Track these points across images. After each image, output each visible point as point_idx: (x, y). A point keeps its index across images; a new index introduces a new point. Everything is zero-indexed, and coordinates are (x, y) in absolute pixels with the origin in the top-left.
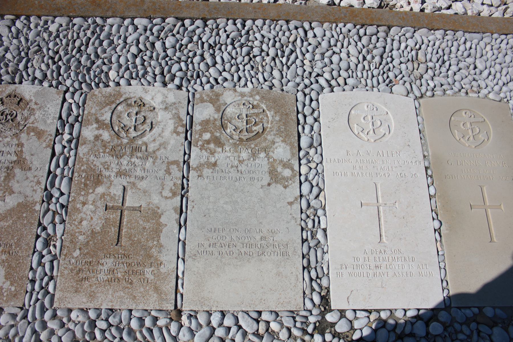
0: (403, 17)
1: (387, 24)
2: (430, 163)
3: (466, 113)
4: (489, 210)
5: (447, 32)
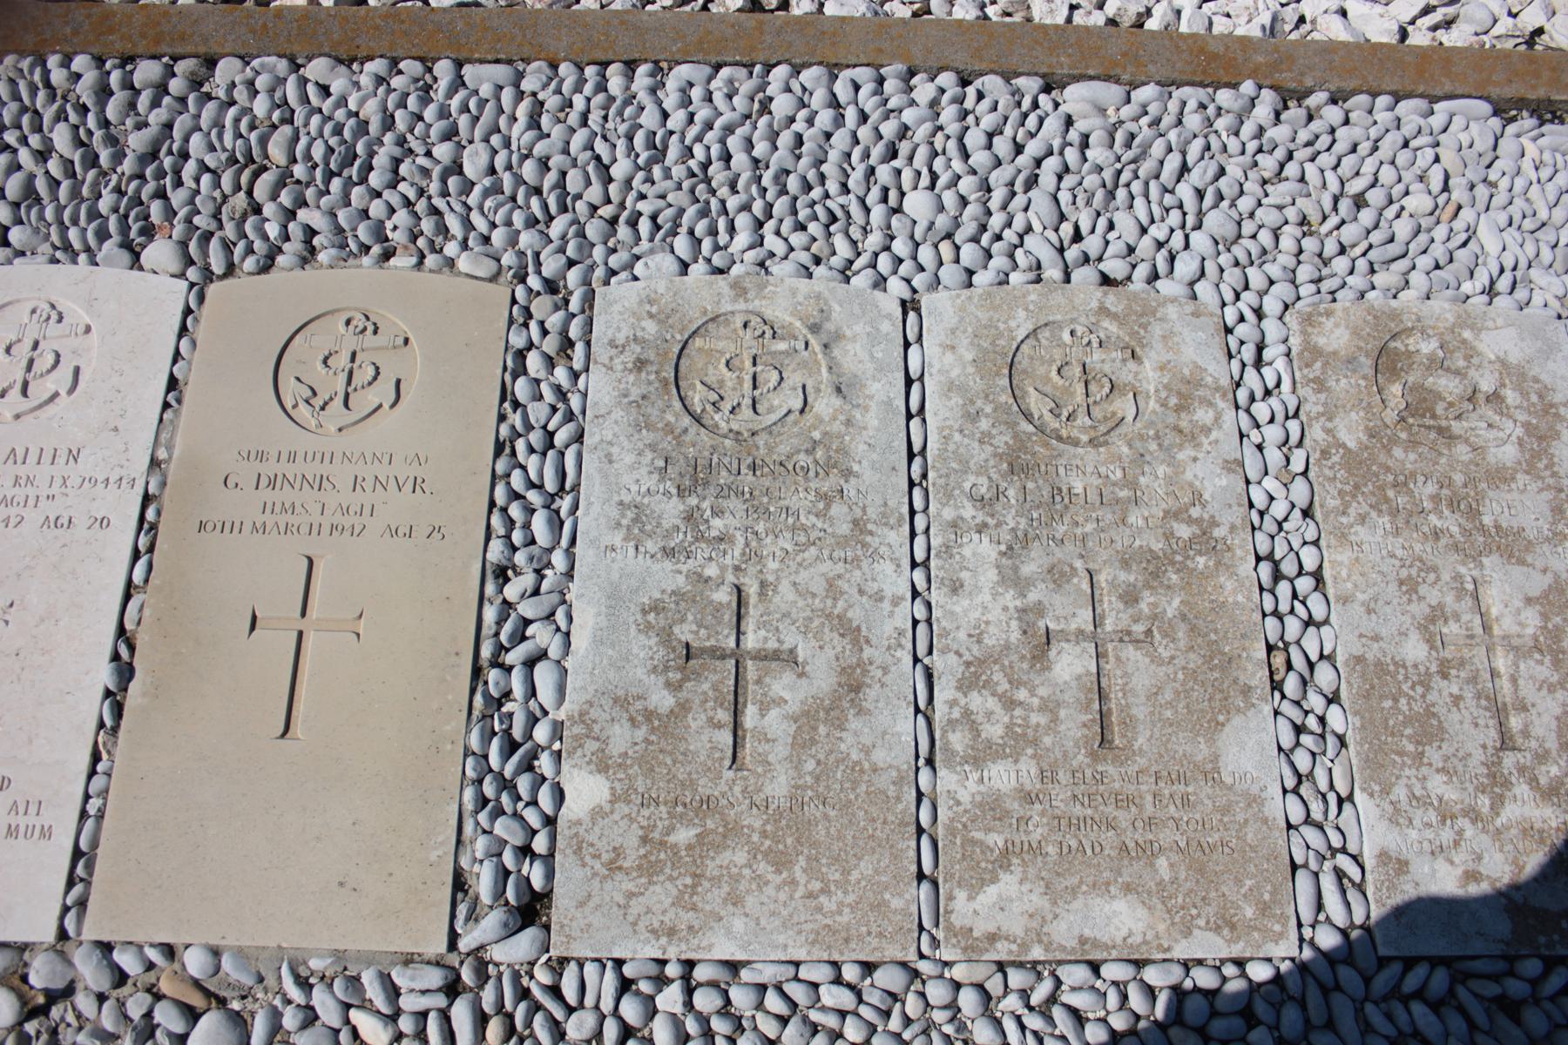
0: (265, 25)
1: (202, 50)
2: (164, 484)
5: (402, 65)
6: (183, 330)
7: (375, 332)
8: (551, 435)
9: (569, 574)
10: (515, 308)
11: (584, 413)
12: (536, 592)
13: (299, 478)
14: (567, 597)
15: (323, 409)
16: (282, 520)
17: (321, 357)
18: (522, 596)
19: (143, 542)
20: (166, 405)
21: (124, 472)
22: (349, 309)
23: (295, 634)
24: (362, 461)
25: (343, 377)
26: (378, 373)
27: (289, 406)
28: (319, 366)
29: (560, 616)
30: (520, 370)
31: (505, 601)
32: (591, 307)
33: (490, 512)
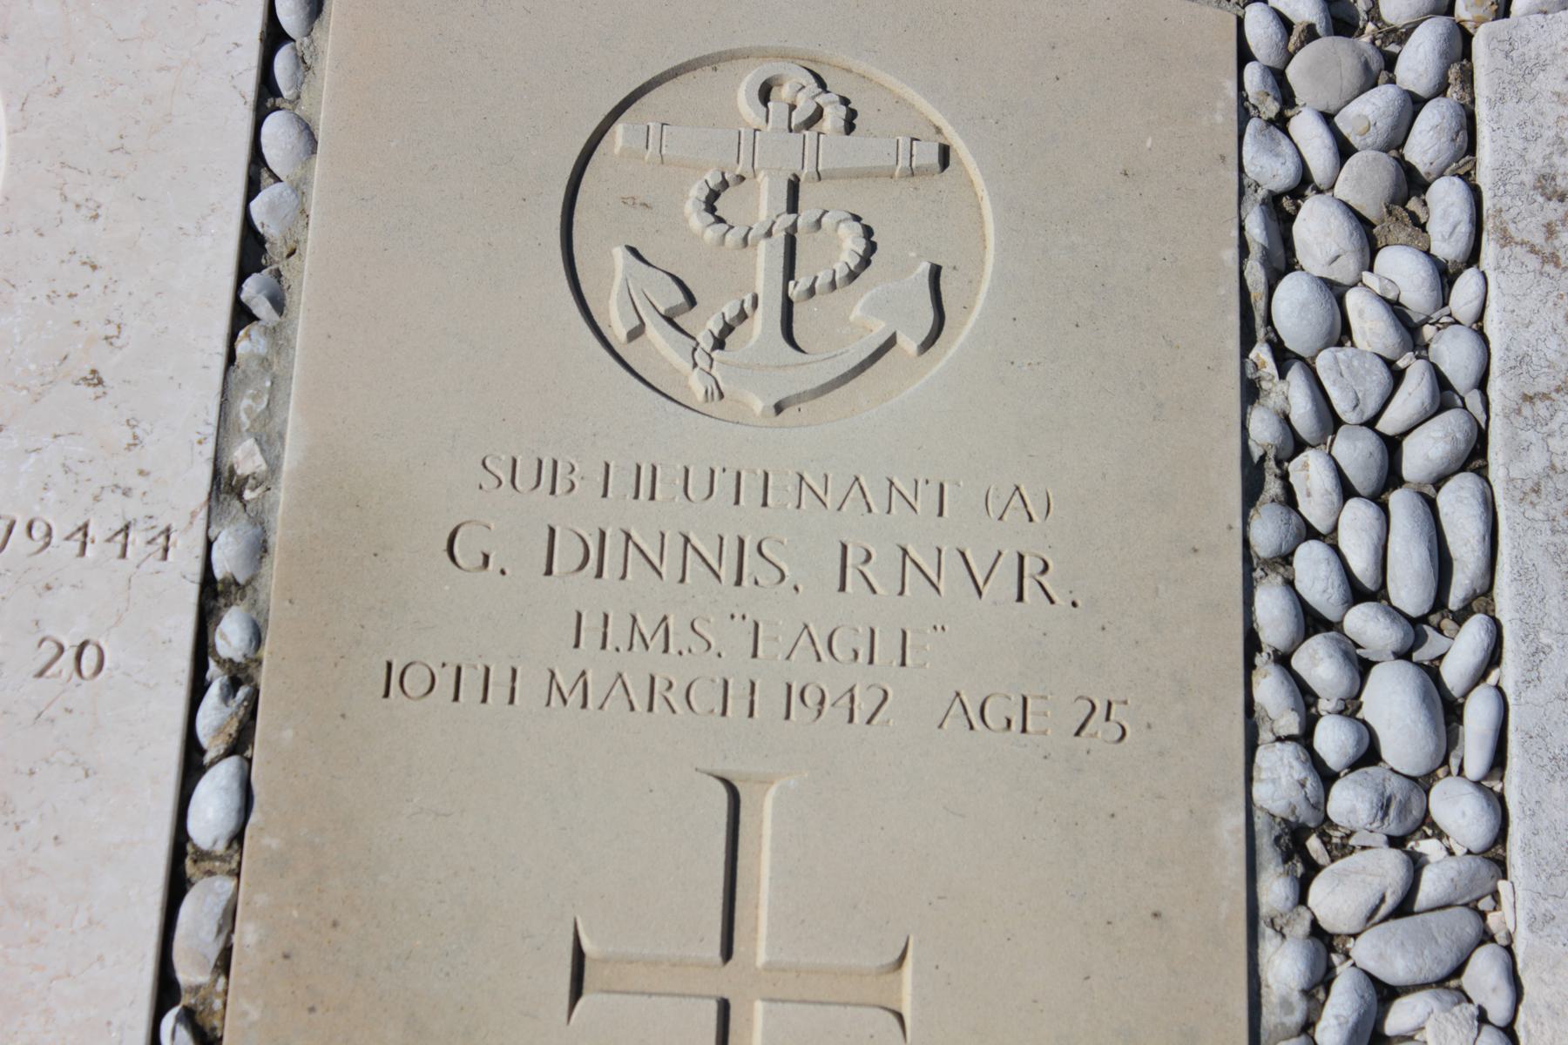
2: (261, 549)
3: (765, 93)
4: (759, 1006)
6: (268, 90)
7: (850, 127)
8: (1392, 446)
9: (1494, 856)
10: (1252, 73)
11: (1482, 384)
12: (1404, 908)
13: (674, 546)
14: (1493, 920)
15: (719, 343)
16: (638, 666)
17: (697, 192)
18: (1371, 918)
19: (214, 715)
20: (242, 315)
21: (133, 509)
22: (764, 54)
23: (713, 1008)
24: (1016, 515)
25: (768, 256)
26: (872, 248)
27: (617, 331)
28: (696, 219)
29: (1484, 975)
30: (1282, 261)
31: (1317, 931)
32: (1468, 78)
33: (1250, 666)
